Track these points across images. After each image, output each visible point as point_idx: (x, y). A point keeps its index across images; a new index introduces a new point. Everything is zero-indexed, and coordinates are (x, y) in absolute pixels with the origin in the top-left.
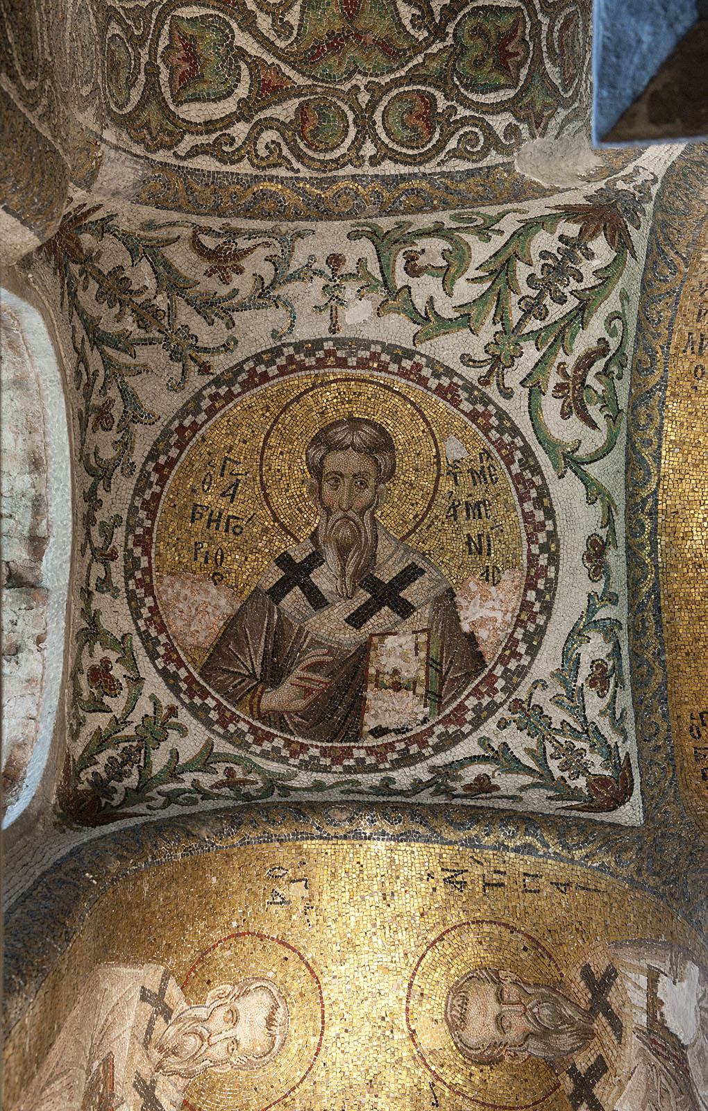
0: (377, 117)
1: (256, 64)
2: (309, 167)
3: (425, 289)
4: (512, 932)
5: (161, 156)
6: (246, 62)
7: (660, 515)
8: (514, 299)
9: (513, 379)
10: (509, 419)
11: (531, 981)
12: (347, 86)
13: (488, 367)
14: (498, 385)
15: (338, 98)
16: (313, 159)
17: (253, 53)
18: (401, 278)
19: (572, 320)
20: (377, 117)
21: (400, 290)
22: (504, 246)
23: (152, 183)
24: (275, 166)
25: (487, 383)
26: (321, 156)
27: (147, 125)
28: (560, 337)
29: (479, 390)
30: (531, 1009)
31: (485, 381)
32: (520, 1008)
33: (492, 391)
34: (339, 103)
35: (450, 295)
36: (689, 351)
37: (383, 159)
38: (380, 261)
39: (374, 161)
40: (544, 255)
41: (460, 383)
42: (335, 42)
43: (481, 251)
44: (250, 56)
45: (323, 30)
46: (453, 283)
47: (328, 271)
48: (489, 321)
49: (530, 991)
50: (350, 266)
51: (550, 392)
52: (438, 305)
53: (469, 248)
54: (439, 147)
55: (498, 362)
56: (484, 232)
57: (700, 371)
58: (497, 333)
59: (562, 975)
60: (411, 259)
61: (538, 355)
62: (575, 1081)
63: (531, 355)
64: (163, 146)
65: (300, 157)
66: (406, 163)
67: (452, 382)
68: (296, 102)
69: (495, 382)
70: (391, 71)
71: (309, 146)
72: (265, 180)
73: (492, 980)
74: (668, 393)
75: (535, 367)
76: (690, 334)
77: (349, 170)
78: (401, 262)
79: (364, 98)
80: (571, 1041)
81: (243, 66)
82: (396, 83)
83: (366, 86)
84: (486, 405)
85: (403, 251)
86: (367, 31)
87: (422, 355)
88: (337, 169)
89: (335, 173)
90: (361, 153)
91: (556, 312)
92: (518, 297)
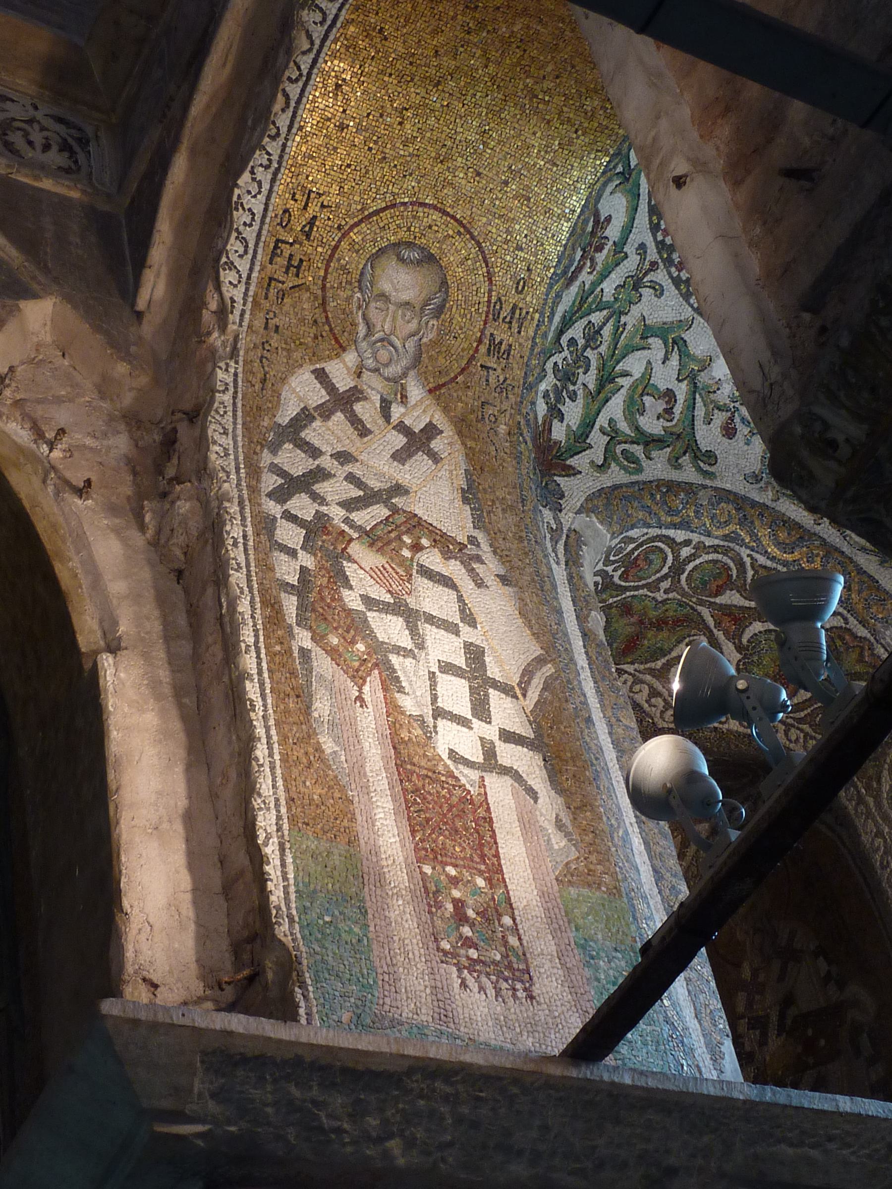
0: (665, 570)
1: (735, 637)
2: (739, 554)
3: (665, 376)
5: (862, 632)
6: (740, 641)
7: (612, 152)
8: (603, 349)
9: (631, 264)
10: (651, 222)
12: (671, 596)
13: (645, 280)
14: (645, 259)
15: (684, 590)
16: (731, 558)
17: (730, 645)
18: (682, 391)
19: (571, 319)
20: (665, 570)
21: (685, 379)
22: (600, 411)
23: (880, 616)
24: (765, 567)
25: (654, 264)
26: (725, 559)
27: (861, 660)
28: (583, 300)
29: (661, 257)
31: (654, 266)
33: (652, 254)
34: (686, 587)
35: (649, 363)
36: (524, 312)
37: (680, 544)
38: (693, 416)
39: (687, 543)
40: (573, 397)
41: (673, 269)
42: (660, 624)
43: (615, 408)
44: (734, 643)
45: (665, 634)
46: (643, 375)
47: (737, 419)
48: (628, 327)
50: (720, 418)
51: (611, 243)
52: (661, 354)
53: (624, 412)
54: (641, 545)
55: (636, 283)
56: (613, 434)
57: (520, 288)
58: (626, 314)
60: (669, 411)
61: (603, 286)
63: (609, 287)
64: (855, 637)
65: (741, 565)
66: (668, 537)
67: (679, 271)
68: (718, 600)
69: (647, 263)
70: (633, 596)
71: (729, 569)
72: (779, 560)
74: (552, 270)
75: (610, 272)
76: (519, 332)
77: (708, 542)
78: (678, 409)
79: (665, 585)
81: (744, 641)
82: (636, 588)
83: (659, 590)
84: (663, 242)
85: (674, 423)
86: (633, 624)
87: (692, 306)
88: (718, 546)
89: (722, 543)
90: (693, 551)
91: (576, 331)
92: (600, 350)
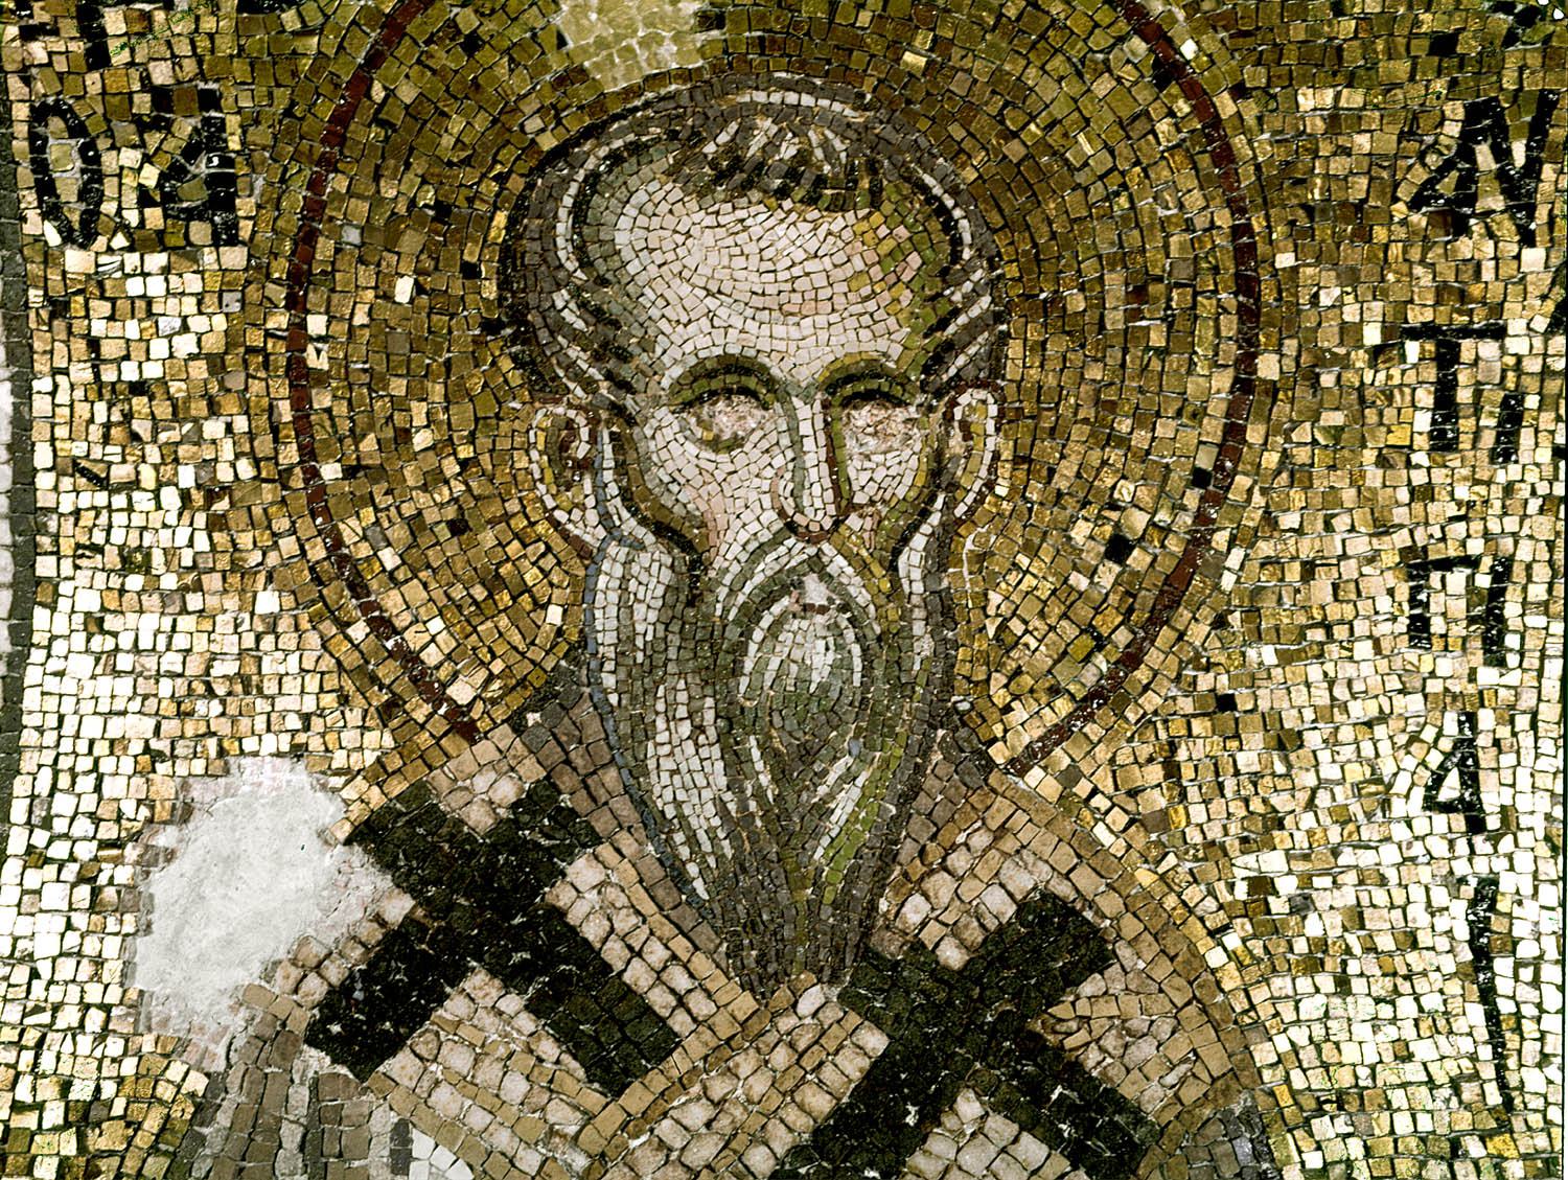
4: (1199, 478)
11: (962, 579)
30: (816, 565)
32: (818, 507)
49: (912, 561)
59: (1019, 765)
62: (506, 835)
73: (950, 348)
80: (704, 817)
